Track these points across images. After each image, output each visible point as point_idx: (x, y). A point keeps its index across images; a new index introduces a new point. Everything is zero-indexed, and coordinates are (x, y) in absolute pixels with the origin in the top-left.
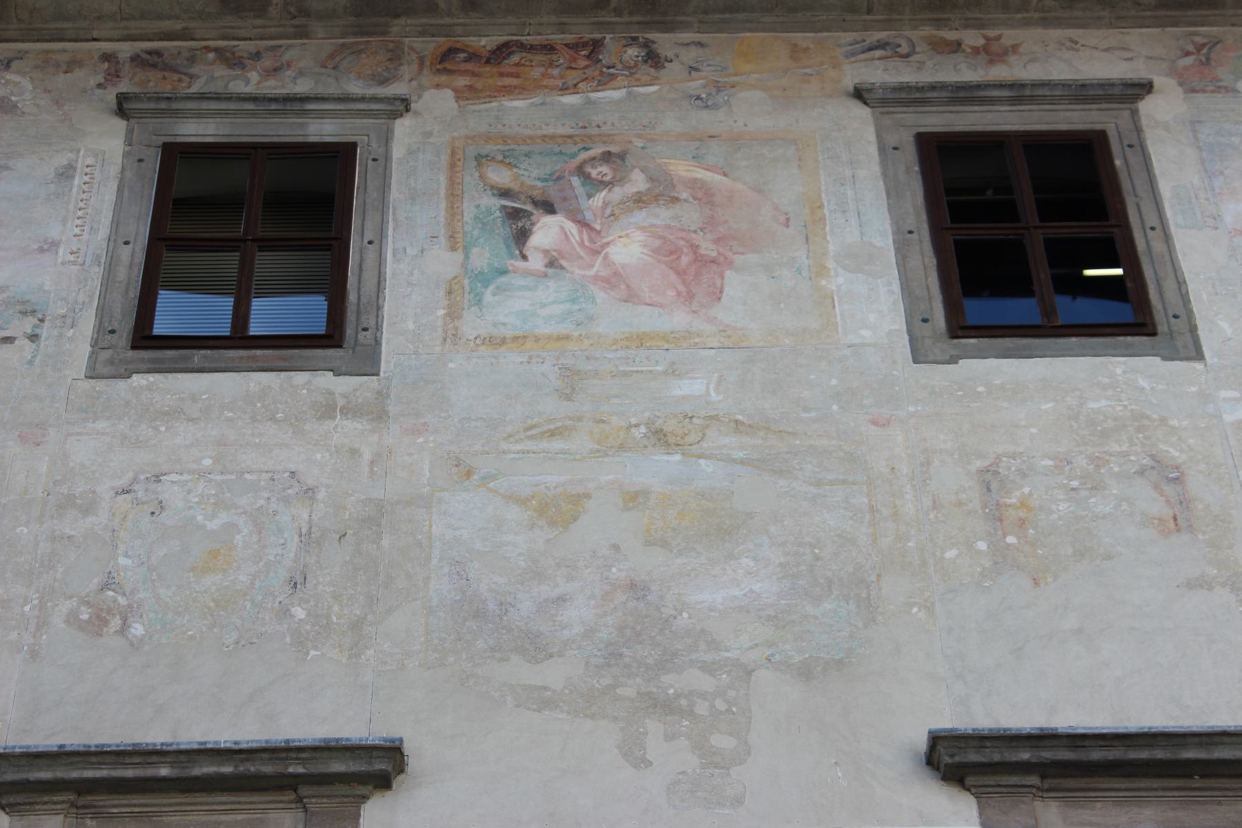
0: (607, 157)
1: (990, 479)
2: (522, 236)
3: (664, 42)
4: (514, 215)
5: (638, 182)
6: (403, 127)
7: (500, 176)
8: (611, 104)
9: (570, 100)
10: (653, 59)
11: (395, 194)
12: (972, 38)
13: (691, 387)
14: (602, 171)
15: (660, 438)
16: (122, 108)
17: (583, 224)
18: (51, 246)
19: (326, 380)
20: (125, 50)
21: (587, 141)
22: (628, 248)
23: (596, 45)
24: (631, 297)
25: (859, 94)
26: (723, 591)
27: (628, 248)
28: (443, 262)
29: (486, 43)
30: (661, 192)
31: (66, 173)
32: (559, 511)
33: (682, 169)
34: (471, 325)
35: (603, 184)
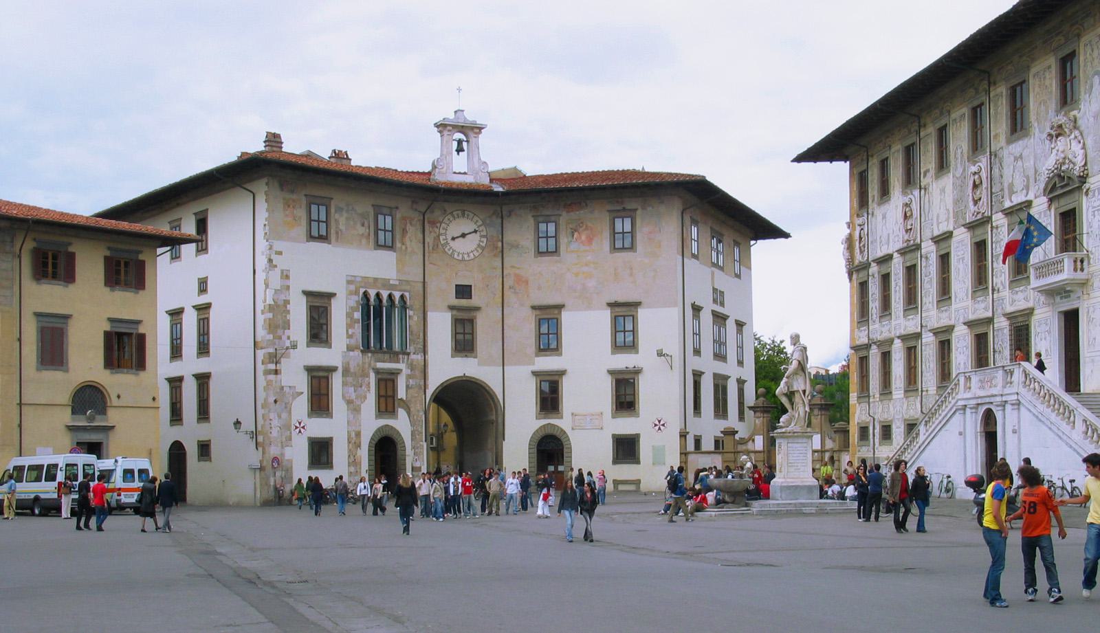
0: (582, 223)
1: (616, 269)
2: (573, 236)
3: (588, 202)
4: (573, 232)
5: (585, 226)
6: (561, 218)
7: (571, 226)
8: (581, 214)
9: (578, 213)
10: (586, 205)
11: (561, 230)
12: (620, 200)
13: (589, 258)
14: (581, 225)
15: (586, 265)
16: (533, 216)
17: (579, 233)
18: (528, 239)
19: (555, 258)
20: (532, 205)
21: (579, 219)
22: (583, 237)
23: (580, 203)
24: (584, 245)
25: (608, 211)
26: (591, 284)
27: (583, 237)
28: (566, 240)
29: (569, 202)
30: (587, 228)
31: (528, 227)
32: (577, 275)
33: (589, 224)
34: (569, 250)
35: (581, 227)
